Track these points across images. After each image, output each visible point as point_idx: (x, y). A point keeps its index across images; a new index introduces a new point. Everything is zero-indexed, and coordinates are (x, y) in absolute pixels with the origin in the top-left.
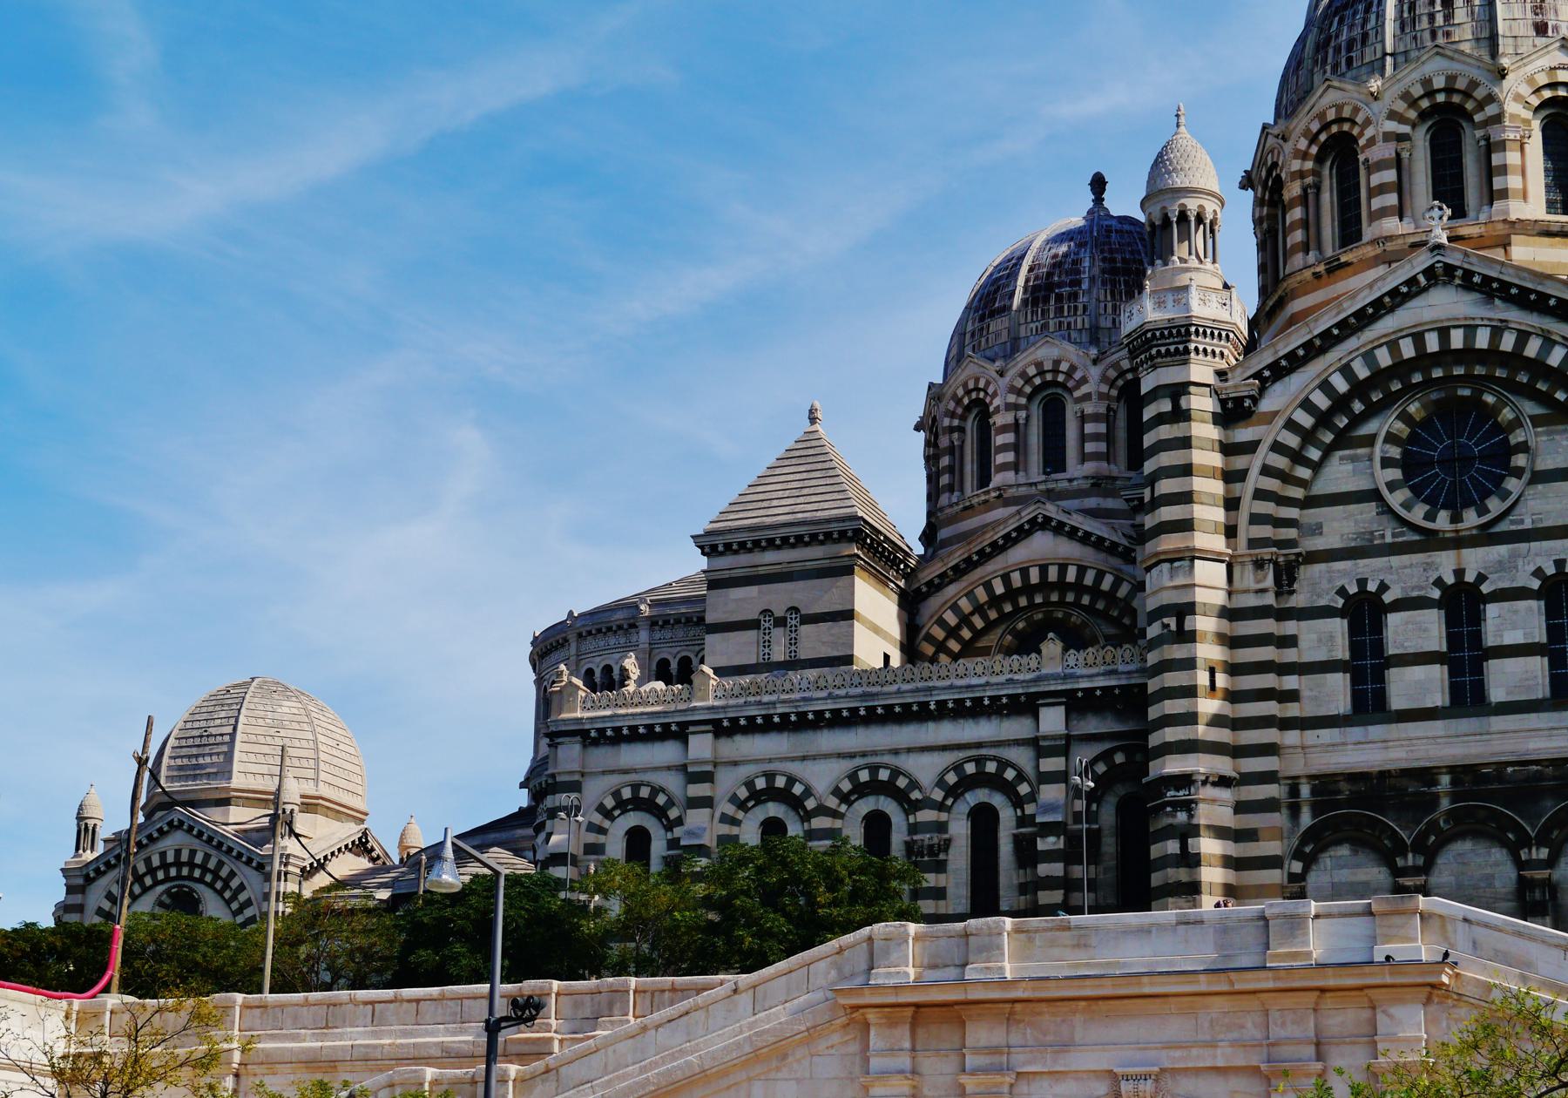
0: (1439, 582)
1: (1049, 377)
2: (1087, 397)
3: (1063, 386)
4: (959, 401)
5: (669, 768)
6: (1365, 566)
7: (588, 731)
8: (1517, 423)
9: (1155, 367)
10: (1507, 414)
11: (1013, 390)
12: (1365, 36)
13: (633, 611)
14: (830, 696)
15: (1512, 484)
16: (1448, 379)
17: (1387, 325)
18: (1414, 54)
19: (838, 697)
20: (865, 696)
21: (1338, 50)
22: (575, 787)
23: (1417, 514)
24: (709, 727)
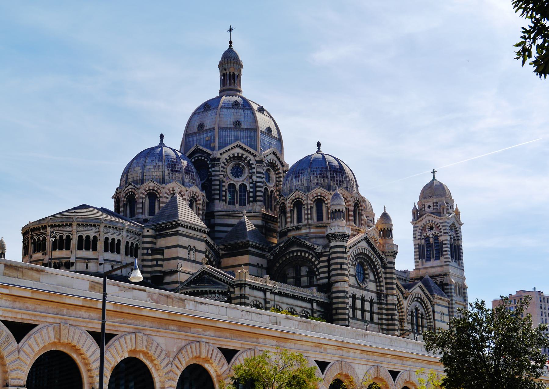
0: (361, 296)
1: (194, 195)
2: (200, 204)
3: (195, 199)
4: (170, 191)
5: (262, 298)
6: (355, 289)
7: (251, 285)
8: (367, 270)
9: (343, 241)
10: (366, 267)
11: (188, 196)
12: (343, 181)
13: (123, 225)
14: (286, 290)
15: (367, 280)
16: (363, 258)
17: (359, 245)
18: (351, 190)
19: (287, 290)
20: (291, 291)
21: (337, 181)
22: (248, 298)
23: (359, 282)
24: (269, 291)
